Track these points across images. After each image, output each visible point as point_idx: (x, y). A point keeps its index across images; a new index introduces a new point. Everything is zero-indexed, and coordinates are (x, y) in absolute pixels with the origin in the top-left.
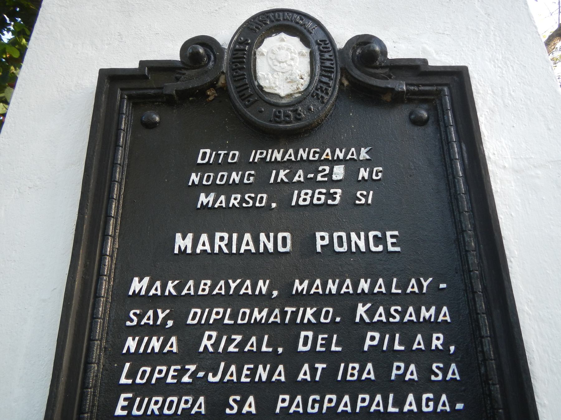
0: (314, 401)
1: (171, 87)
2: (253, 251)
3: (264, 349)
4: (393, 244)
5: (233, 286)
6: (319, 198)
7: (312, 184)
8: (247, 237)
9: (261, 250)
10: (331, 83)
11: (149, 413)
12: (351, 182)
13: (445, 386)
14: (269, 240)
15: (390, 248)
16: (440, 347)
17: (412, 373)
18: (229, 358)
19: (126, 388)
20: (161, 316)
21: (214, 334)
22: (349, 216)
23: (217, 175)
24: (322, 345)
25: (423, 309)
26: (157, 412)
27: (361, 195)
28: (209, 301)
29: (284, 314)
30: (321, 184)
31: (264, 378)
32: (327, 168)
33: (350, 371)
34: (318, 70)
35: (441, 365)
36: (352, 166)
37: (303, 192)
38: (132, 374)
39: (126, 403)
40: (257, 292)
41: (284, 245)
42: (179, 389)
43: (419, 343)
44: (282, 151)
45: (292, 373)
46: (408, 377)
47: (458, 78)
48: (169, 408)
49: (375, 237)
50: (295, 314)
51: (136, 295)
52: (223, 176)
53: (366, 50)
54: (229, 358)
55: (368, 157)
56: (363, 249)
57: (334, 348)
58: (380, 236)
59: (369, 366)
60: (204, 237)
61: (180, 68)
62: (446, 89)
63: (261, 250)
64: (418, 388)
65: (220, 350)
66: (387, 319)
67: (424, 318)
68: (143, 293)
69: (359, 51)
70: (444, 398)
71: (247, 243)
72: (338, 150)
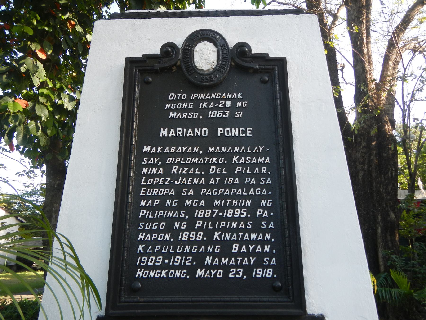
0: (215, 191)
1: (157, 66)
2: (192, 136)
4: (249, 133)
5: (184, 149)
6: (220, 114)
7: (217, 109)
8: (190, 130)
9: (196, 135)
10: (226, 64)
11: (153, 194)
12: (233, 108)
13: (266, 186)
14: (199, 132)
15: (248, 135)
17: (253, 181)
18: (183, 176)
19: (144, 186)
20: (156, 160)
21: (177, 167)
23: (177, 104)
26: (156, 194)
27: (238, 113)
28: (175, 155)
29: (204, 160)
30: (221, 109)
31: (196, 183)
32: (224, 102)
33: (229, 181)
34: (221, 59)
35: (264, 179)
36: (234, 101)
37: (213, 112)
38: (146, 181)
39: (144, 191)
40: (194, 152)
41: (205, 133)
42: (164, 186)
43: (257, 170)
44: (205, 94)
45: (207, 181)
46: (251, 183)
47: (281, 62)
48: (161, 193)
49: (242, 130)
50: (209, 160)
51: (146, 153)
52: (180, 105)
53: (242, 49)
54: (183, 176)
55: (241, 97)
56: (237, 135)
57: (223, 172)
58: (244, 130)
59: (237, 179)
60: (172, 130)
61: (160, 57)
62: (276, 68)
63: (196, 135)
64: (255, 187)
65: (180, 173)
66: (245, 162)
68: (148, 152)
69: (239, 50)
70: (264, 190)
71: (190, 132)
72: (228, 94)
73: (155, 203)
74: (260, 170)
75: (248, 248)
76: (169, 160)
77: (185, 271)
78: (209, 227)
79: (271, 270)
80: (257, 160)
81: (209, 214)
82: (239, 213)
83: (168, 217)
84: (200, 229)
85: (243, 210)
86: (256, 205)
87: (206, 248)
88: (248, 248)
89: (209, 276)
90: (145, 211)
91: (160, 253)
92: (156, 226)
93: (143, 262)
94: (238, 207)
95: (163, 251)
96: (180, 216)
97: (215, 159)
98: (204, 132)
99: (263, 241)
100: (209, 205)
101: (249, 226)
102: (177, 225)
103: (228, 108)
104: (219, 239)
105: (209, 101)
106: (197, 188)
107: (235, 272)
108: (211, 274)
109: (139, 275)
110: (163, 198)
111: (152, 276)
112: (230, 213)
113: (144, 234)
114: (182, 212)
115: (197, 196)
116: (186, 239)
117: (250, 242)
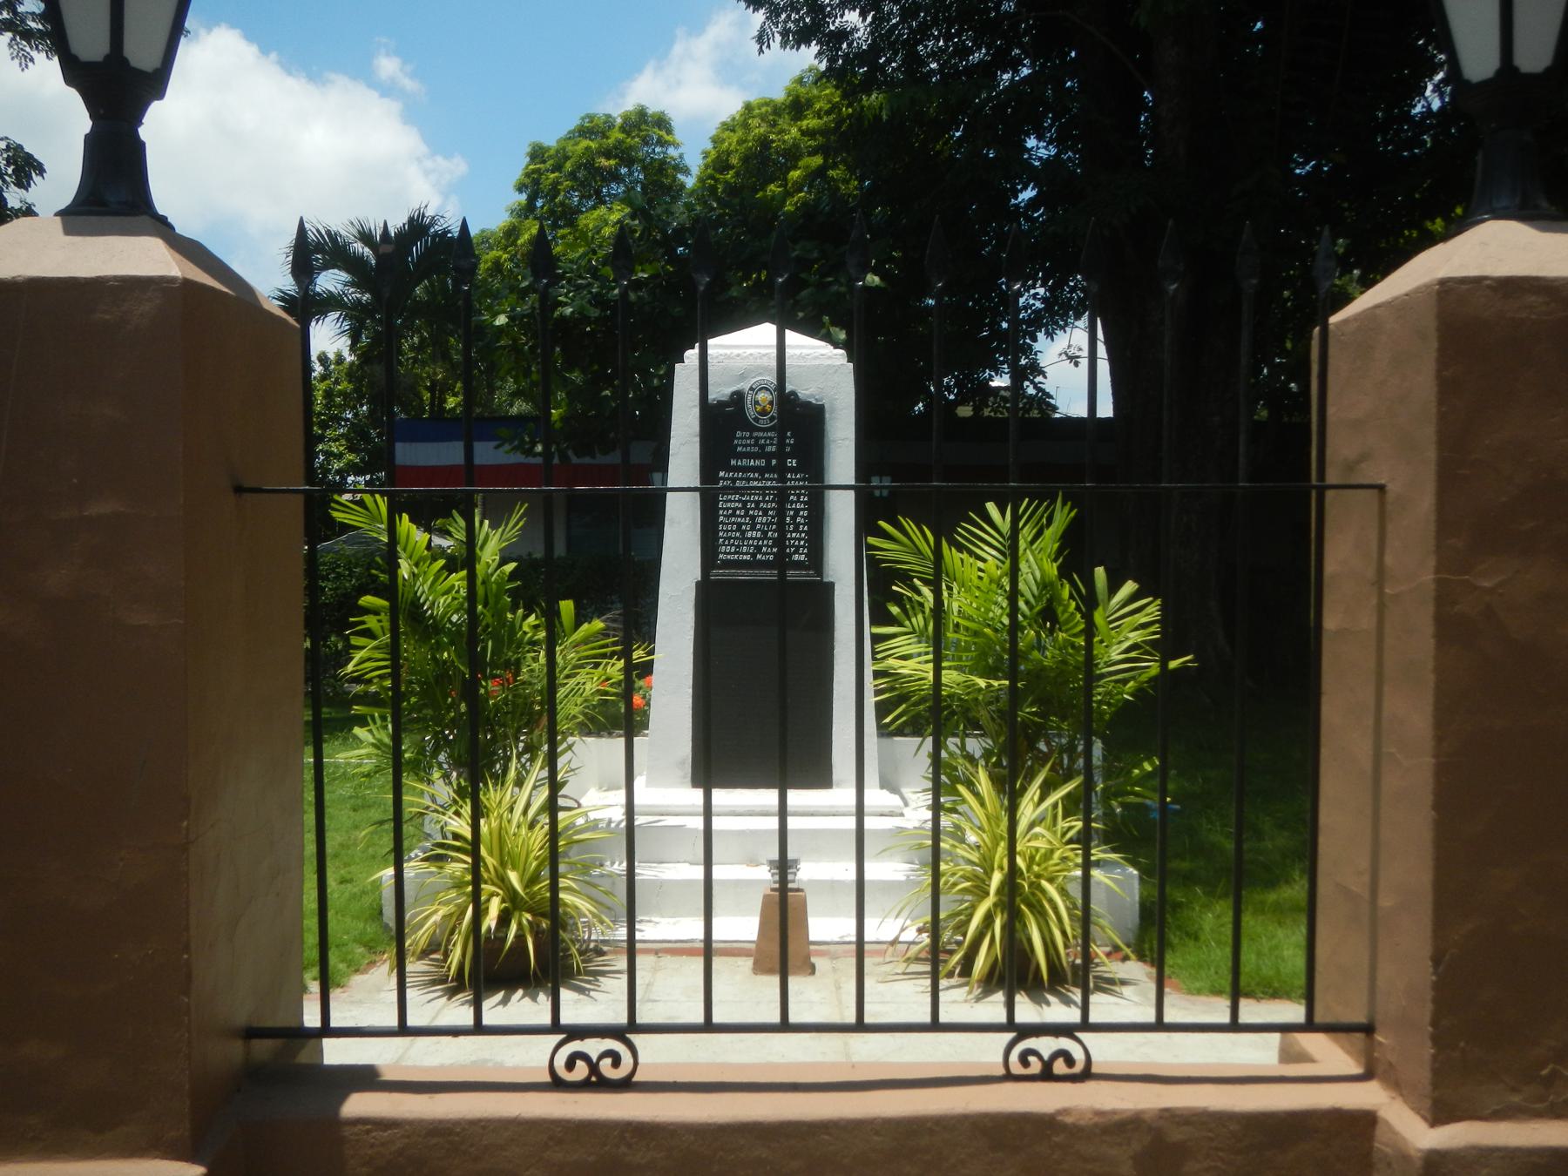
98: (762, 463)
106: (757, 503)
110: (735, 510)
115: (757, 508)
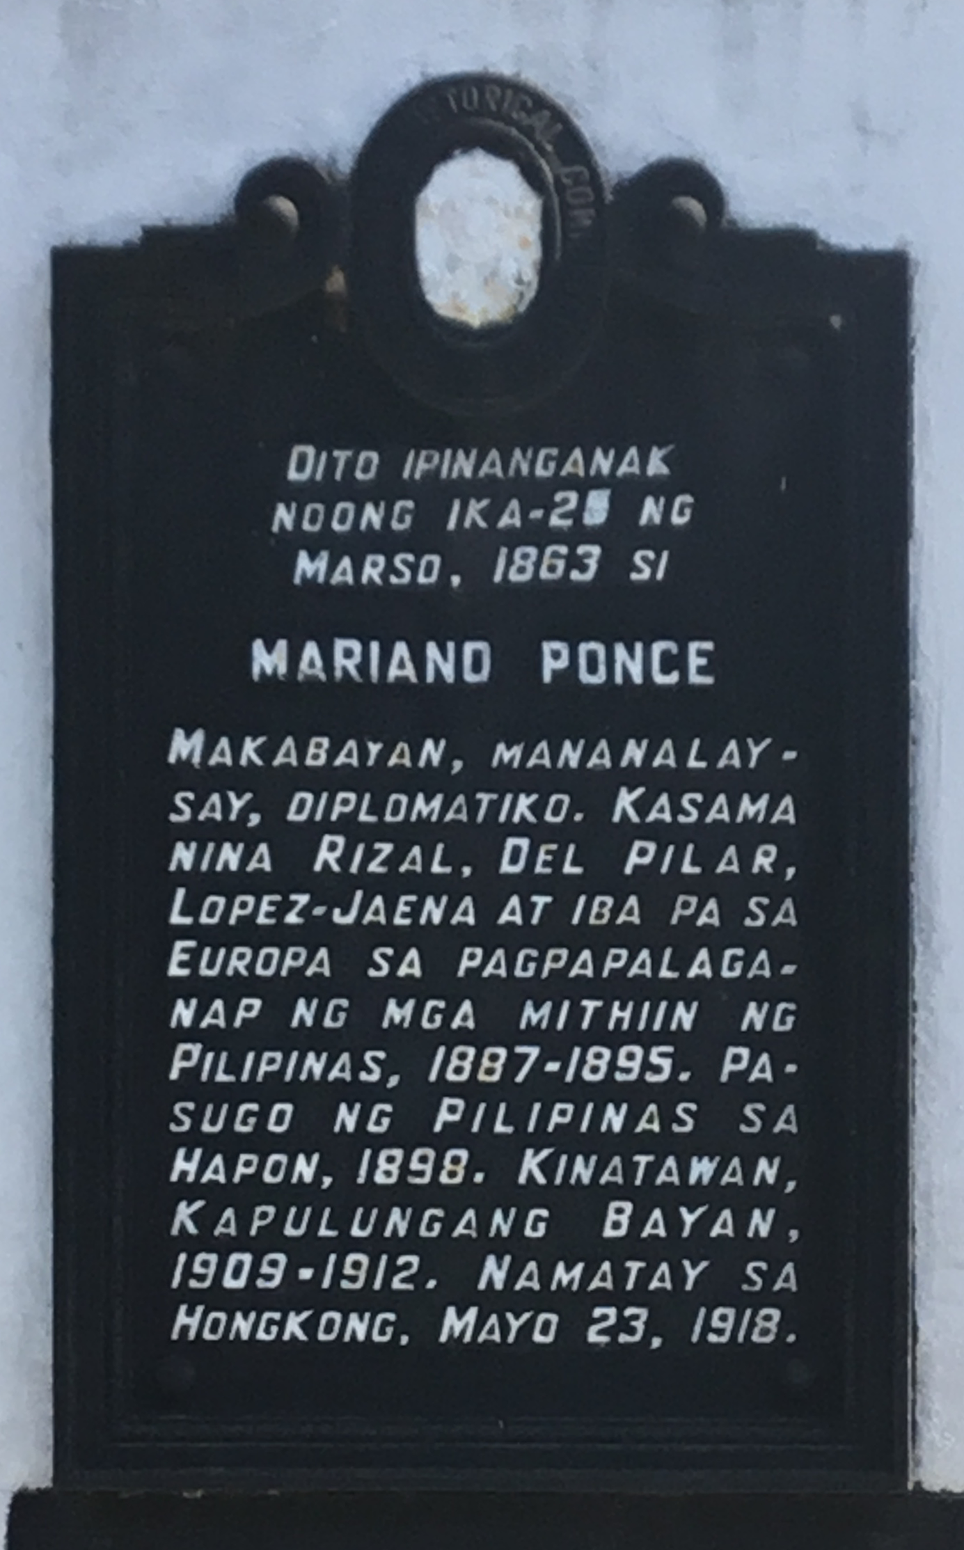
0: (528, 959)
2: (414, 679)
3: (436, 868)
4: (701, 671)
7: (539, 535)
8: (401, 650)
9: (430, 678)
12: (621, 535)
15: (695, 679)
16: (769, 869)
17: (710, 915)
18: (371, 885)
19: (183, 932)
20: (237, 804)
21: (340, 840)
22: (610, 611)
24: (546, 864)
25: (746, 799)
26: (244, 972)
27: (645, 559)
28: (327, 781)
29: (473, 806)
30: (558, 536)
32: (573, 497)
36: (626, 496)
38: (191, 908)
39: (186, 957)
40: (422, 763)
42: (280, 936)
43: (729, 862)
44: (474, 453)
45: (488, 909)
49: (665, 655)
50: (495, 807)
51: (185, 764)
54: (371, 885)
56: (637, 678)
57: (568, 869)
59: (633, 901)
63: (430, 678)
64: (716, 941)
67: (745, 816)
70: (763, 955)
71: (401, 665)
73: (241, 1014)
74: (746, 859)
75: (673, 1223)
76: (301, 807)
77: (391, 1317)
78: (499, 1128)
79: (776, 1314)
80: (734, 806)
81: (499, 1066)
82: (636, 1065)
83: (303, 1077)
84: (456, 1135)
85: (655, 1051)
86: (719, 1024)
87: (484, 1221)
88: (673, 1223)
89: (497, 1337)
90: (196, 1049)
91: (271, 1239)
92: (252, 1120)
93: (201, 1278)
94: (633, 1036)
95: (289, 1231)
96: (363, 1076)
97: (524, 802)
99: (746, 1190)
100: (497, 1026)
101: (682, 1123)
102: (347, 1118)
103: (591, 536)
104: (541, 1179)
105: (496, 492)
106: (440, 944)
107: (612, 1321)
108: (505, 1327)
109: (185, 1329)
110: (281, 993)
111: (245, 1336)
112: (594, 1064)
113: (198, 1153)
114: (368, 1056)
115: (440, 982)
116: (393, 1180)
117: (689, 1194)
